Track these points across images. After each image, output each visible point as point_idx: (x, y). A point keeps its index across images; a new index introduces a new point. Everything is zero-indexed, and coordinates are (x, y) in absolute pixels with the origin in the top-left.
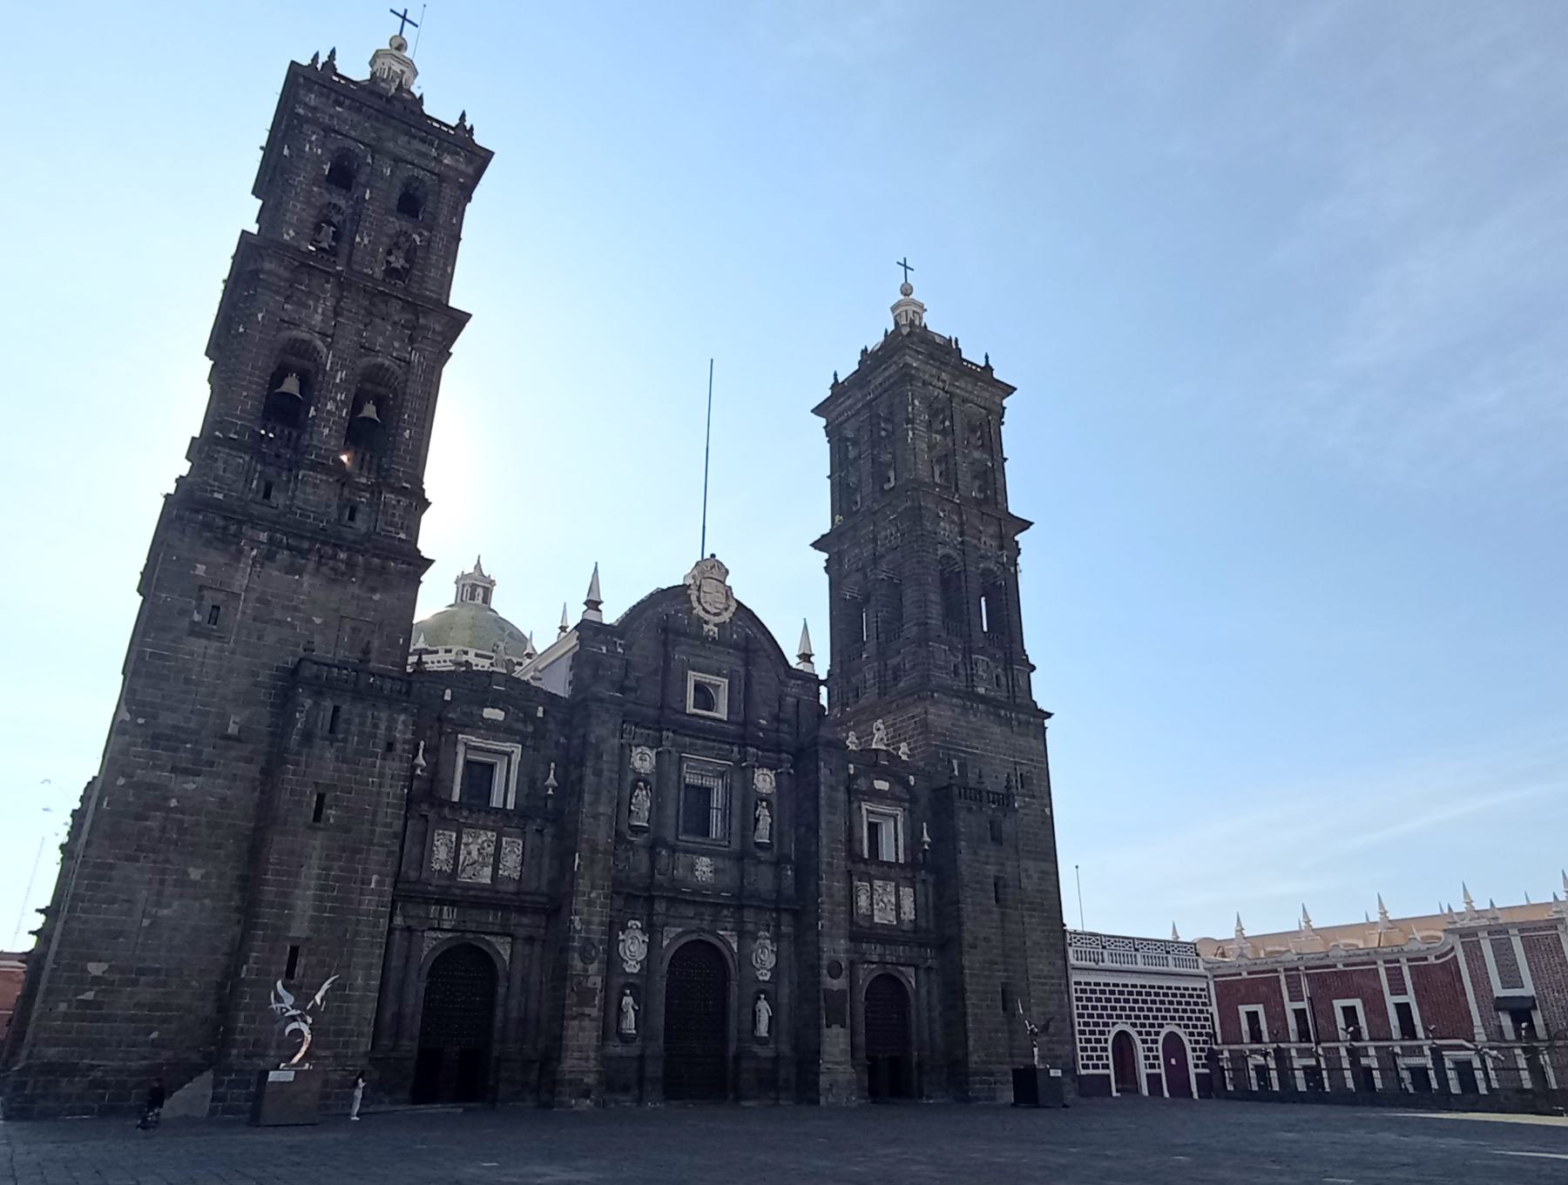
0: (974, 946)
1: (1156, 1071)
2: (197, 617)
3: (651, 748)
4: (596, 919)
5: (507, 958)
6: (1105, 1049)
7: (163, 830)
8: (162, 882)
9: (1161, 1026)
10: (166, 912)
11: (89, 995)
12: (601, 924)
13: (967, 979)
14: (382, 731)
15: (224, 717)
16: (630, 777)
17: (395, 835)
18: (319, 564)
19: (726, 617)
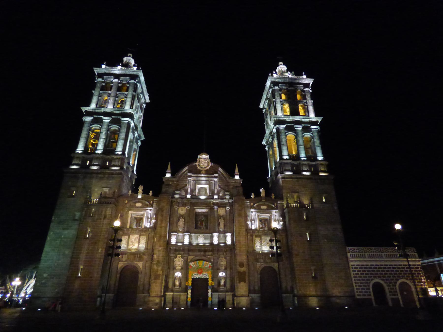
0: (297, 255)
1: (396, 297)
2: (69, 194)
3: (185, 207)
4: (161, 255)
5: (141, 267)
6: (369, 289)
7: (60, 243)
8: (59, 255)
9: (398, 280)
10: (60, 262)
11: (43, 281)
12: (163, 256)
13: (295, 265)
14: (103, 213)
15: (75, 215)
16: (178, 215)
17: (105, 238)
18: (97, 176)
19: (208, 168)
